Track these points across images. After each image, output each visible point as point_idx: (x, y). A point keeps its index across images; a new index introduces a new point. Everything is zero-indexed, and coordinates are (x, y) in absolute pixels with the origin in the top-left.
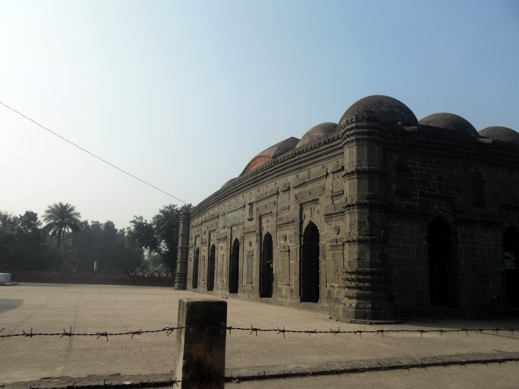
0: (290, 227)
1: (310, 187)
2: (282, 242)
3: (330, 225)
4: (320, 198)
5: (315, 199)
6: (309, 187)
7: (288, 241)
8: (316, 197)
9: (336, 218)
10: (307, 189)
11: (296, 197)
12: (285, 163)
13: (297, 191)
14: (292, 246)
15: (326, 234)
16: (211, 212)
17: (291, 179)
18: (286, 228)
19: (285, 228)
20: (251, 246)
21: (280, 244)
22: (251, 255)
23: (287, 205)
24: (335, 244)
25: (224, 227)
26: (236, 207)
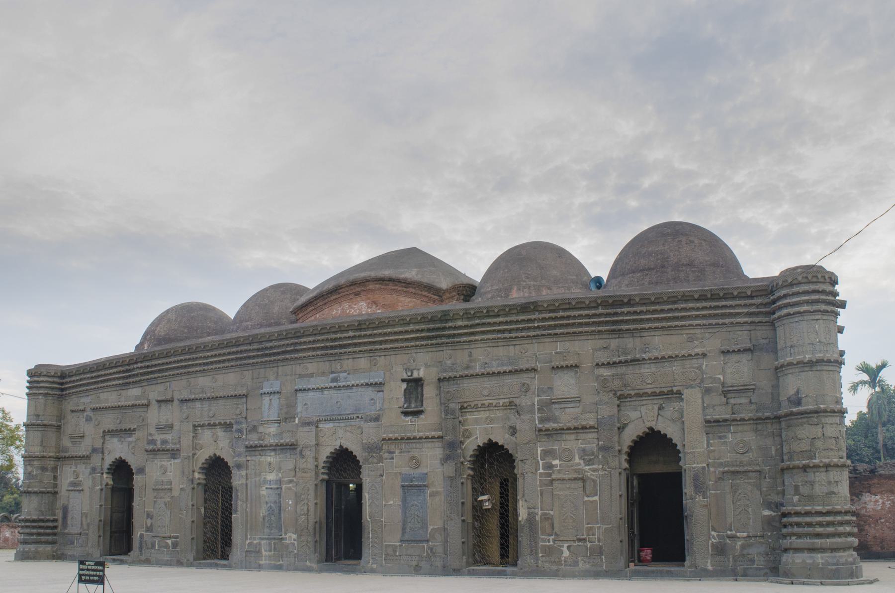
0: (582, 436)
1: (653, 370)
2: (556, 462)
3: (720, 438)
4: (686, 393)
5: (671, 392)
6: (647, 370)
7: (577, 460)
8: (675, 389)
9: (740, 428)
10: (642, 371)
11: (604, 383)
12: (561, 314)
13: (606, 372)
14: (594, 470)
15: (697, 453)
16: (203, 382)
17: (585, 349)
18: (573, 437)
19: (568, 437)
20: (418, 465)
21: (550, 466)
22: (412, 487)
23: (574, 393)
24: (741, 469)
25: (279, 422)
26: (335, 380)
